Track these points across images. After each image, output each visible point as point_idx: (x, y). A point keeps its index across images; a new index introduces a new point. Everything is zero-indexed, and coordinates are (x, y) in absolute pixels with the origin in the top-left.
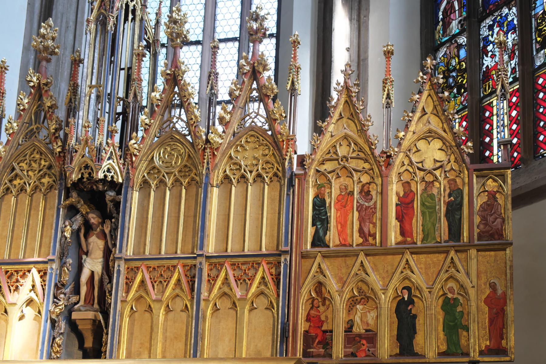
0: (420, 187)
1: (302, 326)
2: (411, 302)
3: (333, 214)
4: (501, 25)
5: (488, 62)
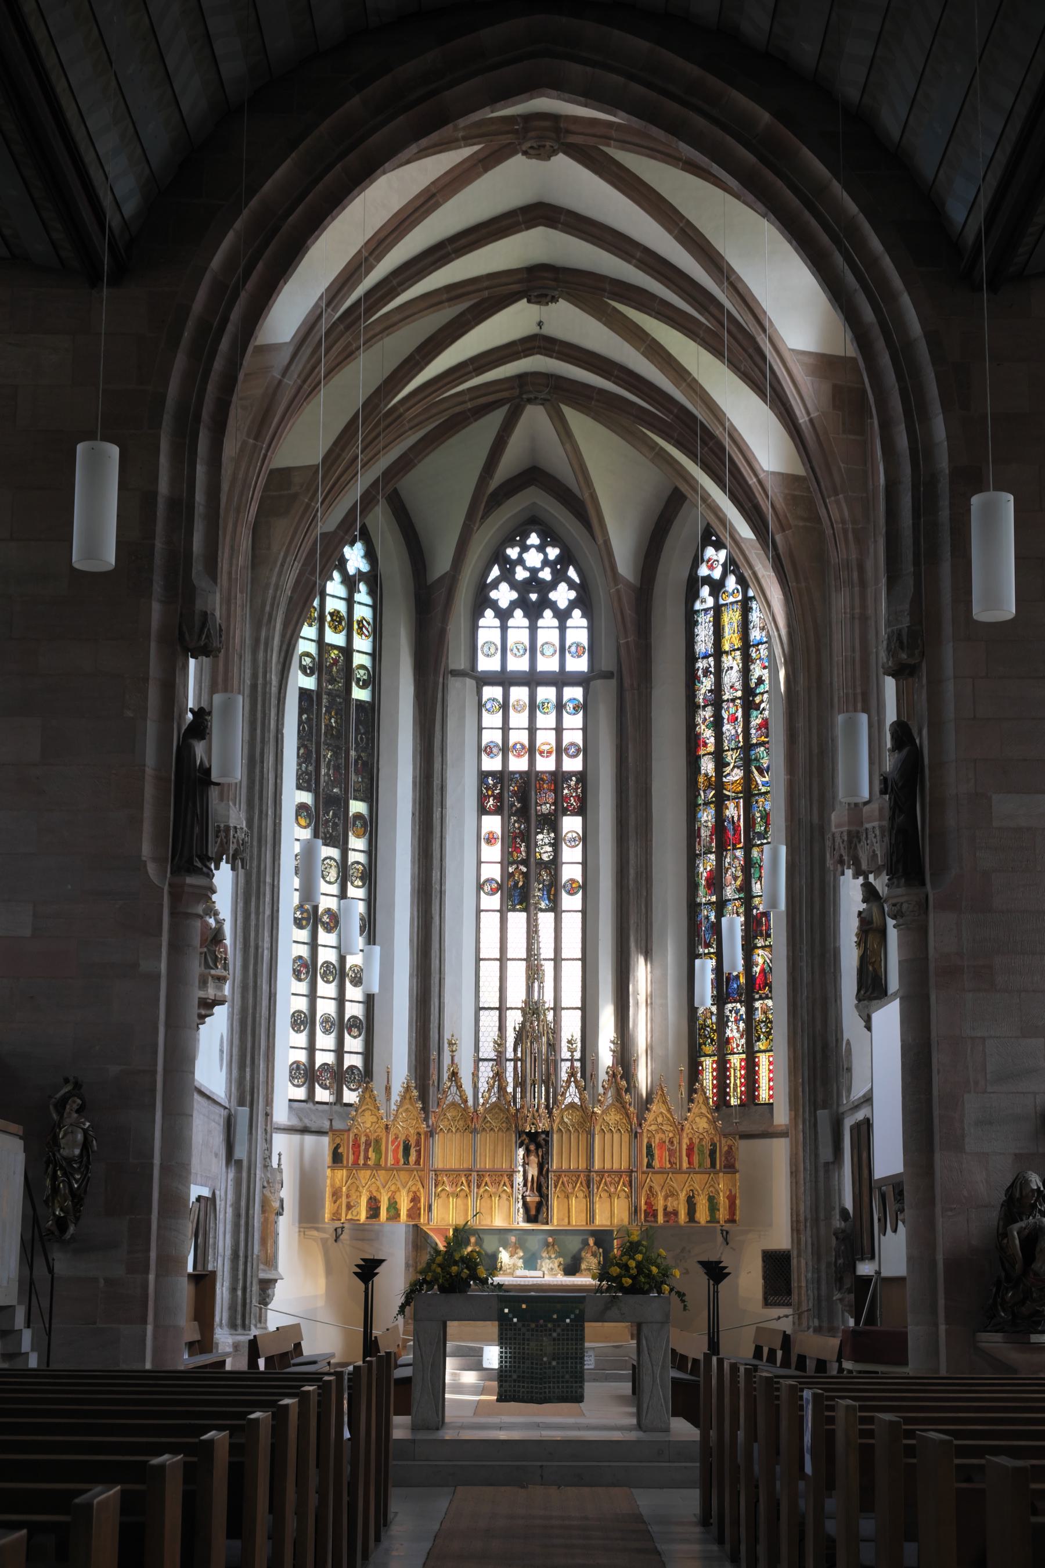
0: (698, 1140)
1: (643, 1207)
2: (693, 1197)
3: (656, 1152)
4: (737, 1013)
5: (728, 1033)
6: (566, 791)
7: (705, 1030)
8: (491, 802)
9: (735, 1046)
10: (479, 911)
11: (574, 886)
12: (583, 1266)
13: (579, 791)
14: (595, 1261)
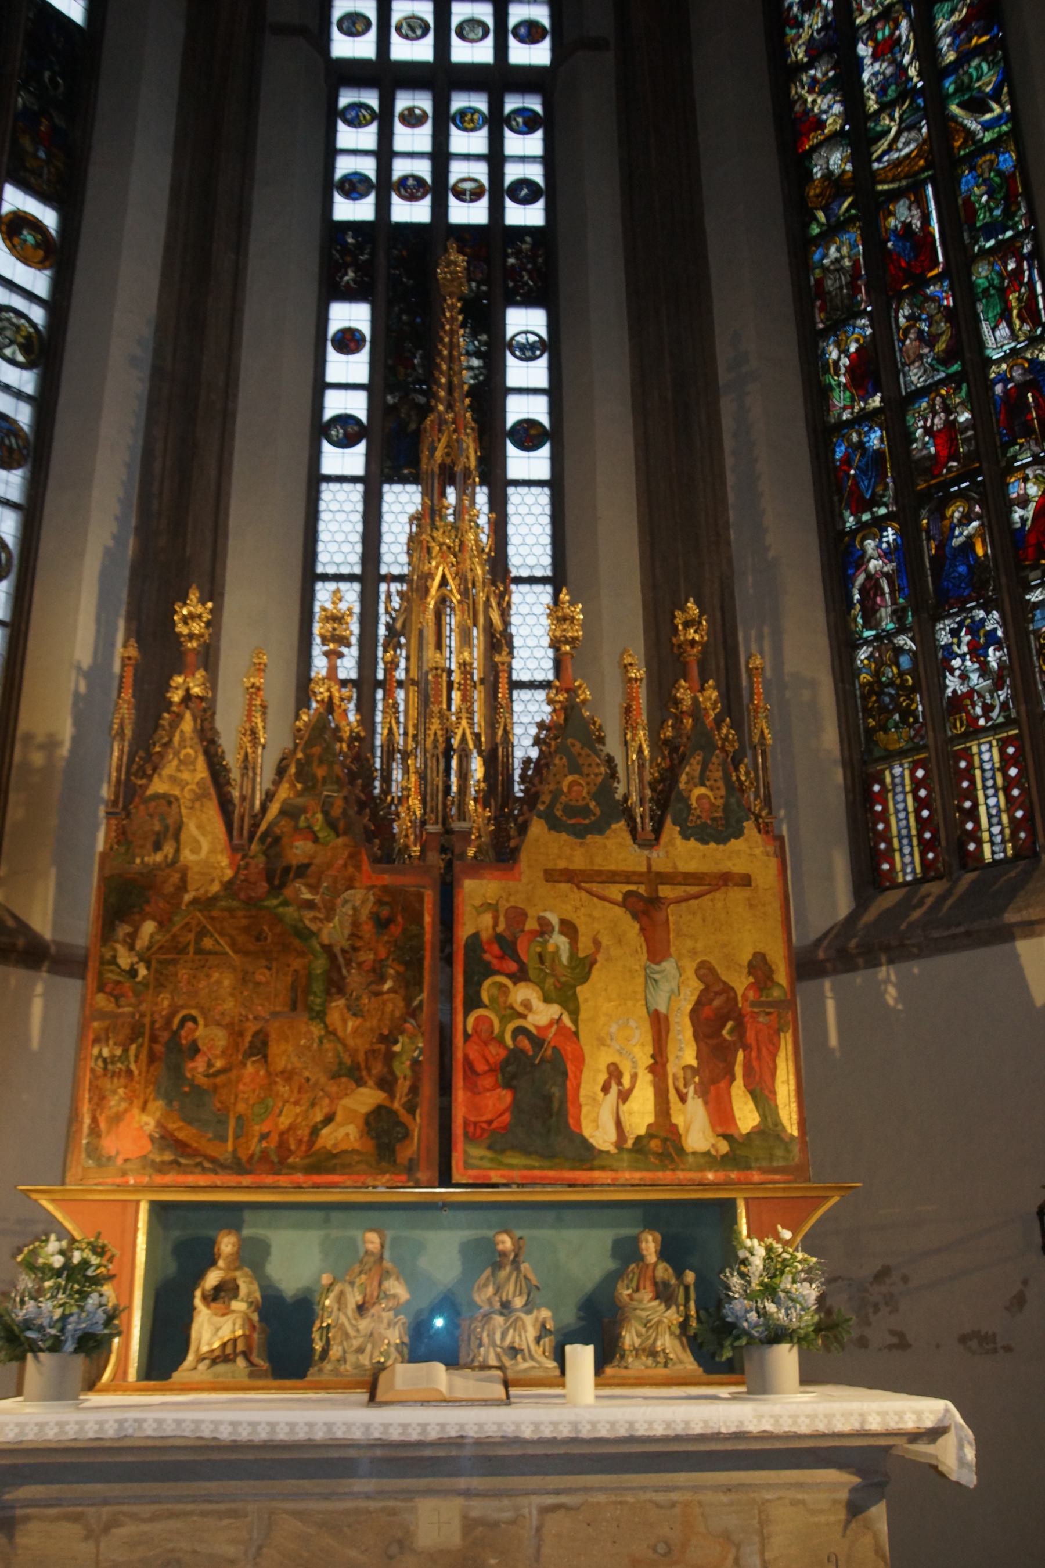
5: (953, 683)
6: (511, 261)
7: (880, 694)
8: (351, 274)
9: (979, 711)
10: (316, 479)
11: (533, 432)
12: (630, 1338)
13: (540, 260)
14: (673, 1316)
